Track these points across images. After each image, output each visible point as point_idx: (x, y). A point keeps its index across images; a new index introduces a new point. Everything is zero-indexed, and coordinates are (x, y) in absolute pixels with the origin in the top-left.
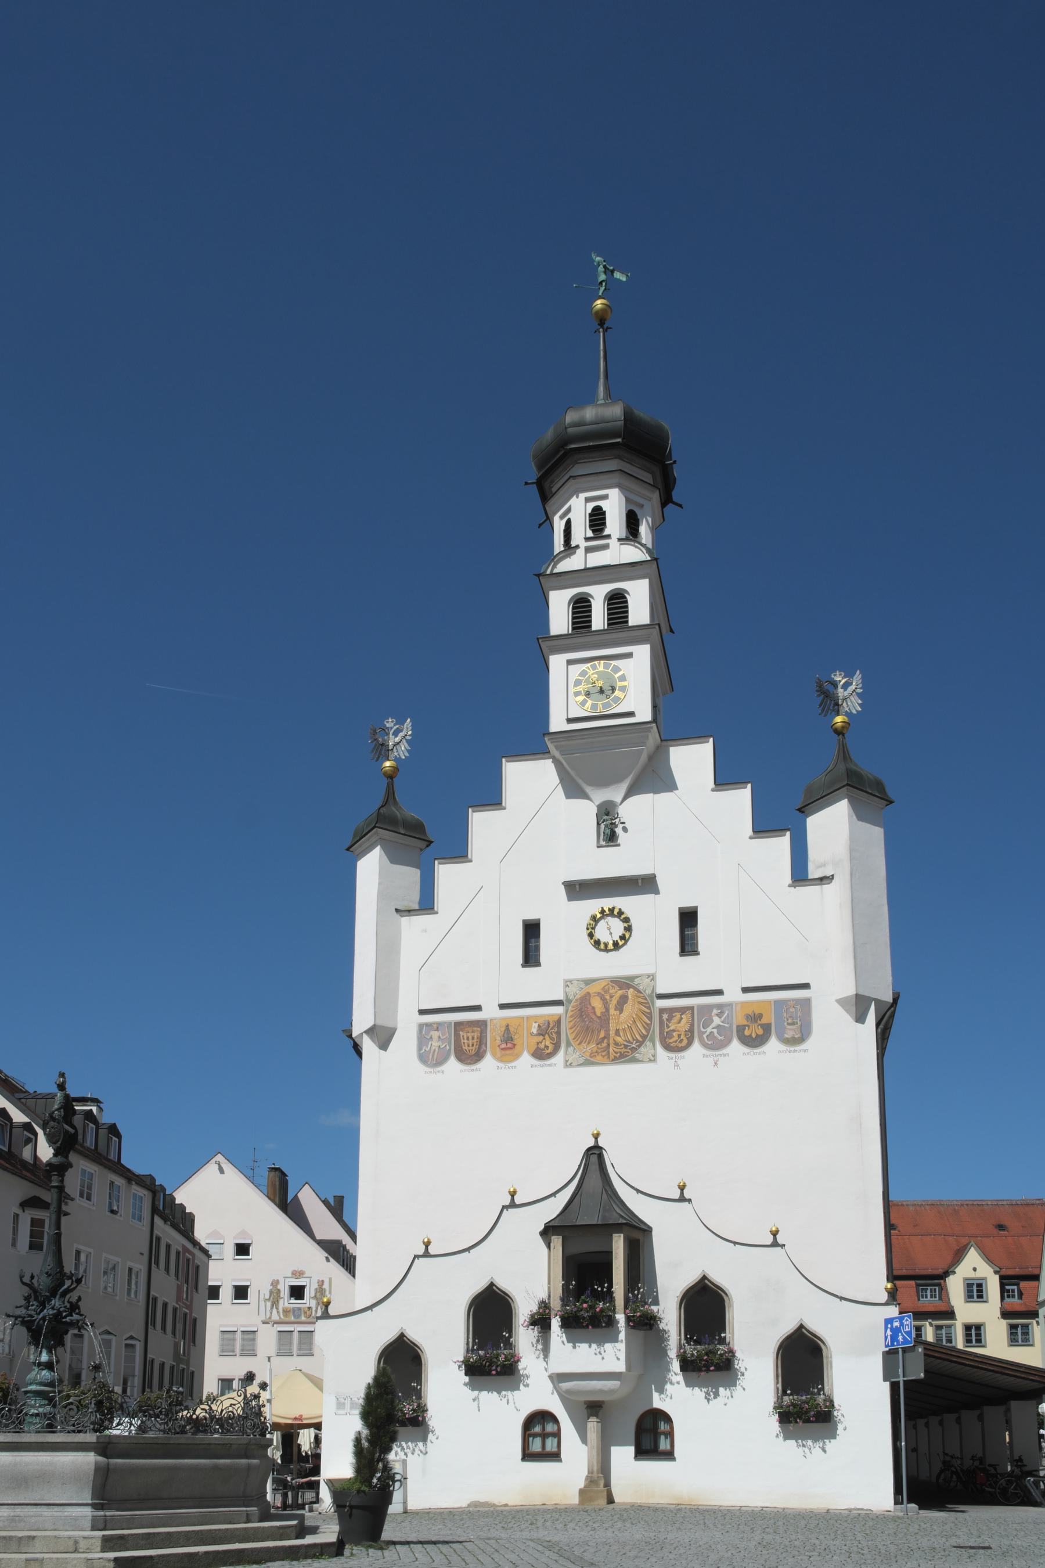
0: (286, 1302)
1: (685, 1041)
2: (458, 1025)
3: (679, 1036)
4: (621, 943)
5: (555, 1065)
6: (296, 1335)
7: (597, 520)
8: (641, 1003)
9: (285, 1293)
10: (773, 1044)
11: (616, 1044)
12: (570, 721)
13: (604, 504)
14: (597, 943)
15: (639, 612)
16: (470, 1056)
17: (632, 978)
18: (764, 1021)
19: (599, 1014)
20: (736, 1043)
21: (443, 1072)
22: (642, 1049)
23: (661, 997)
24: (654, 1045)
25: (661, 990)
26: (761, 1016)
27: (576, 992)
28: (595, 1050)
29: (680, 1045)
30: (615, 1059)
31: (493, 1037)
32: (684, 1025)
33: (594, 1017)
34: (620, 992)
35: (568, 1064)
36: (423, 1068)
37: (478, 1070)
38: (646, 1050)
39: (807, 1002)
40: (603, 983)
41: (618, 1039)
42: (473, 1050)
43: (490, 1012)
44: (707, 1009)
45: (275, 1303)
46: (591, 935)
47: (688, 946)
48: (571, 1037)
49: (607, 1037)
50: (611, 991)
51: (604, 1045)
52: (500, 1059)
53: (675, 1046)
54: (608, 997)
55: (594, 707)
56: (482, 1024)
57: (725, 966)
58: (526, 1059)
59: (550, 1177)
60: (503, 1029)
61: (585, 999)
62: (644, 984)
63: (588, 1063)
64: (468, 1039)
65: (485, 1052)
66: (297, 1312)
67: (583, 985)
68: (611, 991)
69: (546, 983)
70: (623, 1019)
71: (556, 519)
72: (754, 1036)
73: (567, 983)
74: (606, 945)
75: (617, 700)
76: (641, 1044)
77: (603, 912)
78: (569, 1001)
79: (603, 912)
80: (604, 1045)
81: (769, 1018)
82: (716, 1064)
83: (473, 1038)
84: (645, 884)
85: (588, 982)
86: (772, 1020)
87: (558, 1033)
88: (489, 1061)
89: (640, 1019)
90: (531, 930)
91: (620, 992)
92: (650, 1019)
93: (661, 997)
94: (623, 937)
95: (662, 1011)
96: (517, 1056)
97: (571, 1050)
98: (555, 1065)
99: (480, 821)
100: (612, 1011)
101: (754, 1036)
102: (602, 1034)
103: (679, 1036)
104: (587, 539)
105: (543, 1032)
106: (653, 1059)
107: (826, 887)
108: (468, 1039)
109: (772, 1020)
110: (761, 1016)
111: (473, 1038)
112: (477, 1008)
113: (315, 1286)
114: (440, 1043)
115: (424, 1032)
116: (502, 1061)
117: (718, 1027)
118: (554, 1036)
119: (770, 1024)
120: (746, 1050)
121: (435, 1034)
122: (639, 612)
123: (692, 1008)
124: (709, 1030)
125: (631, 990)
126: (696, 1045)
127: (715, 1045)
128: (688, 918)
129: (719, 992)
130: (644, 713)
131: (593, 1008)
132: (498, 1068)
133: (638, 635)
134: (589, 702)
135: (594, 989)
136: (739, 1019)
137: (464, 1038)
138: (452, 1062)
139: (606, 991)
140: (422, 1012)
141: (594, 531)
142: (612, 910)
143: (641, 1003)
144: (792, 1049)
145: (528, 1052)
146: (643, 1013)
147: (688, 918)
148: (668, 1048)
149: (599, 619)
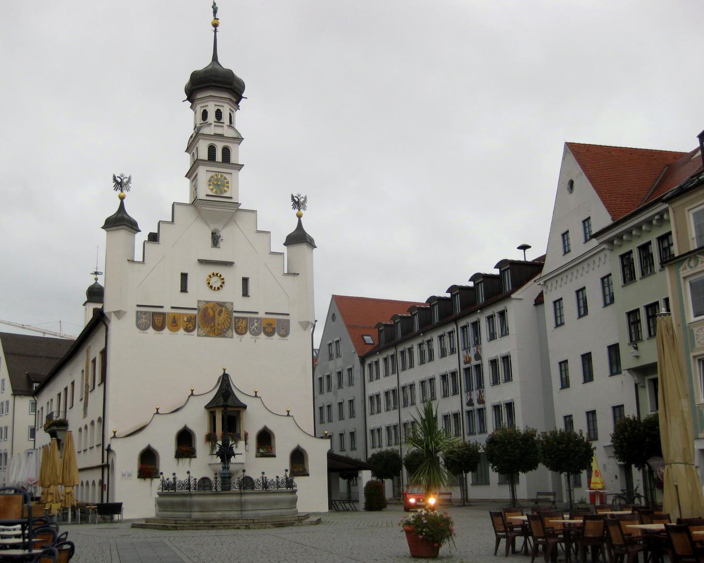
1: (244, 331)
2: (154, 314)
3: (242, 329)
4: (220, 288)
5: (193, 335)
7: (219, 114)
8: (227, 313)
10: (276, 336)
11: (218, 329)
13: (221, 108)
14: (211, 287)
16: (159, 328)
17: (224, 303)
18: (273, 326)
19: (211, 316)
20: (262, 333)
21: (147, 333)
22: (228, 332)
24: (232, 331)
25: (235, 309)
26: (272, 324)
27: (202, 306)
28: (209, 330)
29: (243, 332)
30: (217, 335)
31: (168, 320)
32: (244, 324)
33: (209, 316)
34: (220, 308)
35: (199, 335)
36: (138, 330)
37: (162, 334)
38: (229, 333)
39: (288, 321)
40: (214, 303)
41: (219, 327)
43: (167, 310)
44: (252, 319)
47: (245, 293)
48: (200, 325)
49: (214, 326)
50: (216, 307)
51: (213, 329)
52: (171, 330)
53: (241, 333)
54: (215, 309)
55: (216, 192)
56: (164, 314)
57: (259, 304)
58: (182, 331)
60: (173, 317)
61: (206, 309)
62: (228, 306)
64: (158, 320)
65: (165, 326)
67: (205, 303)
68: (216, 307)
70: (220, 319)
72: (269, 332)
73: (199, 302)
74: (215, 288)
75: (225, 191)
76: (228, 330)
77: (213, 274)
78: (199, 309)
79: (213, 274)
80: (213, 329)
81: (275, 325)
82: (255, 341)
83: (160, 320)
85: (207, 302)
86: (275, 327)
87: (195, 322)
88: (166, 330)
89: (227, 320)
90: (184, 276)
91: (220, 308)
92: (231, 320)
93: (235, 312)
94: (221, 286)
95: (236, 318)
96: (178, 330)
97: (200, 329)
98: (193, 335)
100: (216, 316)
101: (269, 332)
102: (212, 324)
103: (242, 329)
104: (215, 122)
106: (232, 337)
107: (296, 277)
108: (158, 320)
109: (275, 327)
110: (272, 324)
111: (160, 320)
112: (162, 307)
114: (146, 320)
115: (139, 315)
116: (172, 331)
117: (256, 327)
118: (194, 323)
119: (275, 328)
120: (267, 337)
121: (144, 316)
123: (246, 318)
124: (253, 327)
125: (224, 308)
126: (248, 332)
127: (255, 334)
128: (245, 281)
131: (209, 313)
132: (170, 334)
134: (214, 190)
136: (264, 325)
137: (156, 320)
138: (151, 330)
139: (214, 307)
140: (138, 306)
141: (217, 119)
142: (217, 274)
143: (227, 313)
144: (283, 338)
145: (183, 328)
146: (228, 317)
147: (245, 281)
148: (238, 333)
149: (219, 157)
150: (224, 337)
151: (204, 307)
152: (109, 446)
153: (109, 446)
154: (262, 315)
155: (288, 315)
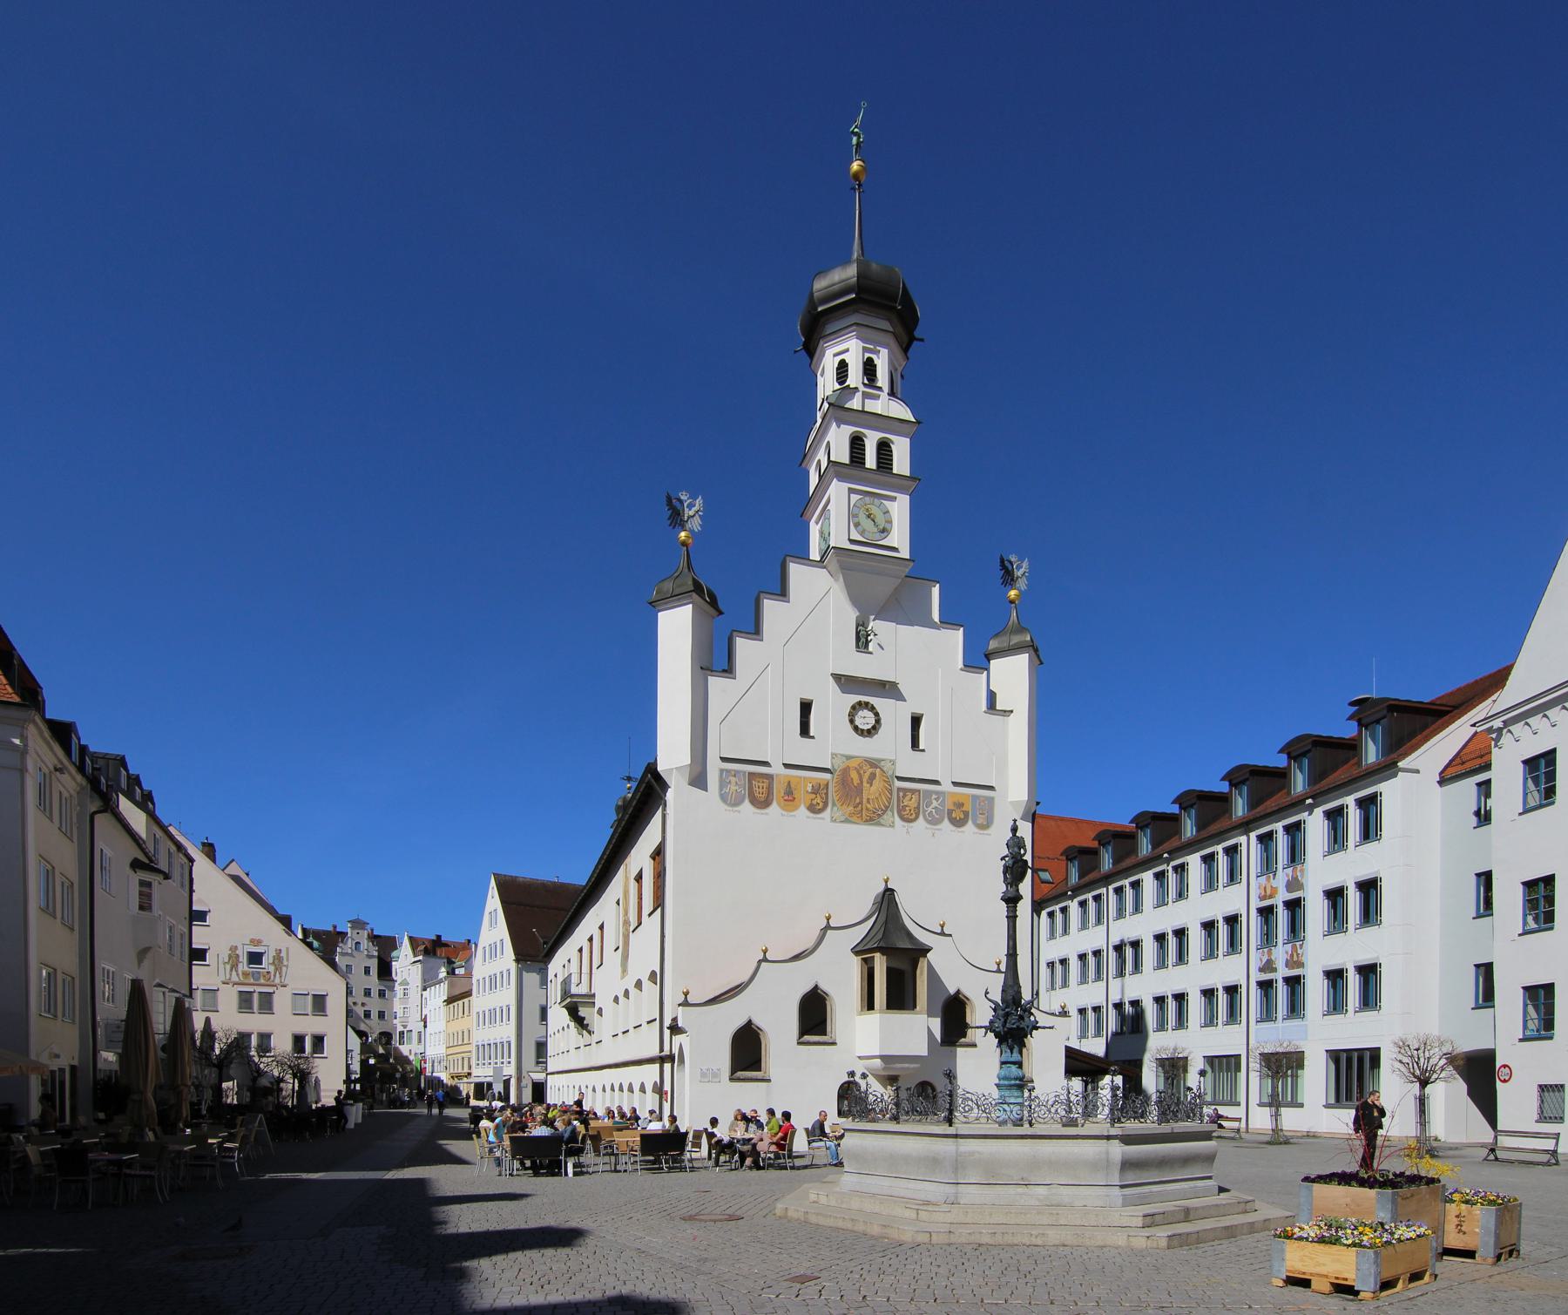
0: (243, 966)
2: (751, 775)
6: (256, 996)
7: (869, 369)
9: (244, 959)
12: (852, 542)
15: (901, 463)
16: (762, 803)
23: (900, 779)
27: (839, 764)
31: (779, 790)
32: (913, 803)
38: (887, 817)
39: (992, 799)
42: (762, 797)
44: (930, 793)
45: (234, 967)
46: (852, 721)
56: (770, 777)
57: (940, 761)
58: (803, 811)
59: (858, 907)
61: (846, 771)
62: (887, 767)
63: (846, 821)
66: (256, 976)
69: (814, 752)
70: (872, 791)
71: (829, 353)
73: (834, 756)
81: (968, 807)
84: (888, 689)
85: (849, 758)
86: (968, 808)
90: (806, 707)
93: (900, 779)
96: (796, 808)
99: (770, 606)
105: (815, 791)
106: (892, 826)
112: (766, 764)
113: (272, 953)
121: (733, 779)
122: (901, 463)
127: (933, 821)
128: (916, 721)
129: (936, 782)
130: (905, 553)
133: (899, 483)
135: (853, 763)
136: (949, 805)
137: (758, 787)
138: (747, 805)
140: (724, 759)
147: (916, 721)
148: (903, 818)
149: (871, 461)
150: (879, 824)
151: (843, 766)
152: (675, 1019)
153: (675, 1019)
154: (946, 786)
155: (991, 788)
